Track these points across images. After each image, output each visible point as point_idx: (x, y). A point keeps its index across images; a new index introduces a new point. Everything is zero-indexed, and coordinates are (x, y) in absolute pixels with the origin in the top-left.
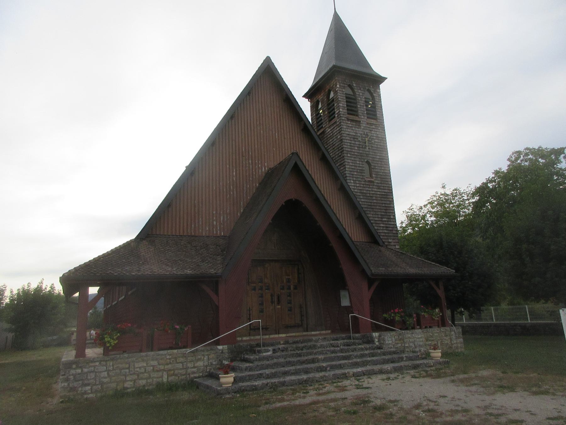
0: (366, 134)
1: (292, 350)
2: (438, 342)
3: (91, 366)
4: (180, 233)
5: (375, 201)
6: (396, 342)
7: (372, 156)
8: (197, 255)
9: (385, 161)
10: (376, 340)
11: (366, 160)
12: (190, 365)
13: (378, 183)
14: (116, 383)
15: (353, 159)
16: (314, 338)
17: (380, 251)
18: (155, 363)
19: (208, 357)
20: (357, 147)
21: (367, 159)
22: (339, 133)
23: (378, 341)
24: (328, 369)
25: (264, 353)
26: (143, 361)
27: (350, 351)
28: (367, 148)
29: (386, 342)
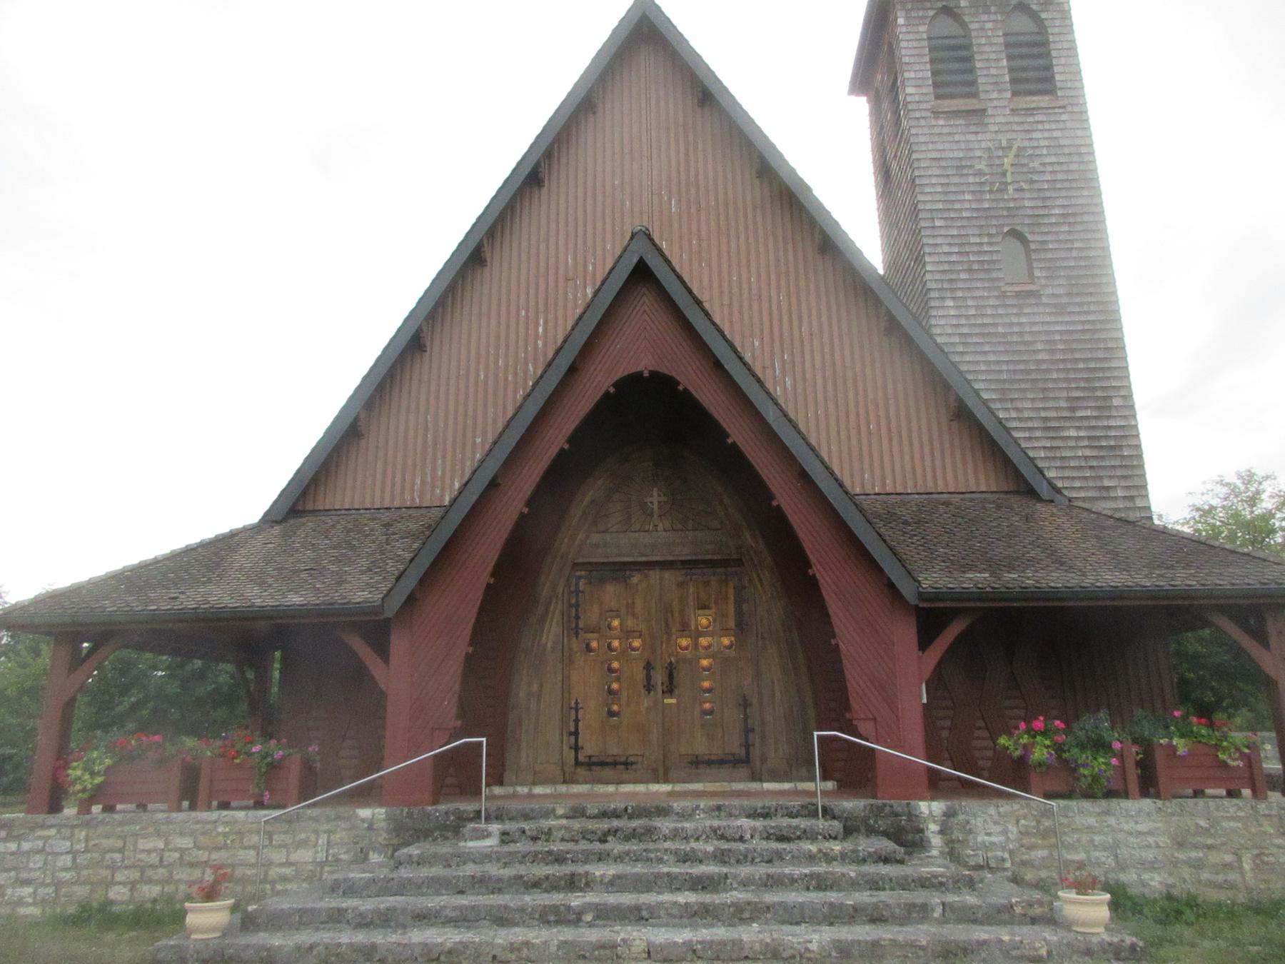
1: (566, 838)
2: (1240, 859)
3: (39, 838)
4: (383, 498)
6: (1026, 841)
10: (933, 827)
12: (278, 856)
14: (89, 887)
16: (677, 805)
18: (186, 842)
19: (329, 837)
21: (1008, 225)
23: (941, 832)
24: (588, 917)
25: (471, 840)
26: (158, 834)
27: (757, 860)
28: (1010, 188)
29: (975, 839)
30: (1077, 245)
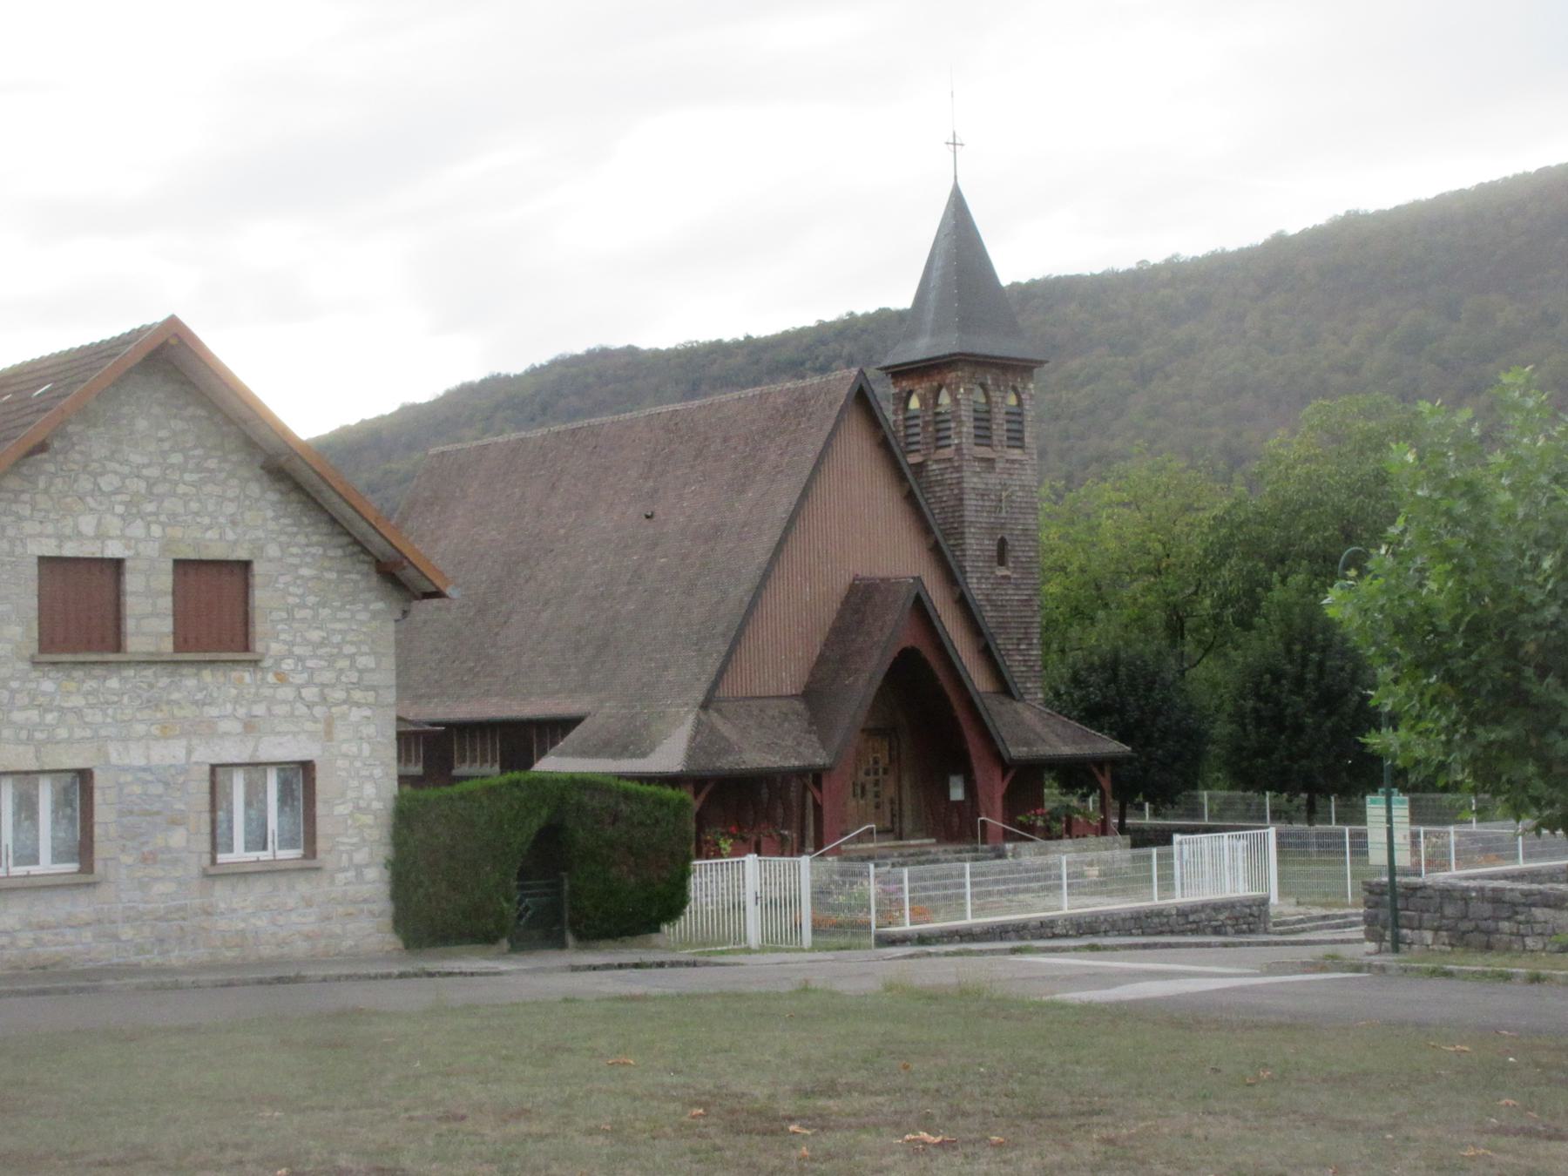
5: (1009, 614)
17: (1016, 712)
28: (1004, 511)
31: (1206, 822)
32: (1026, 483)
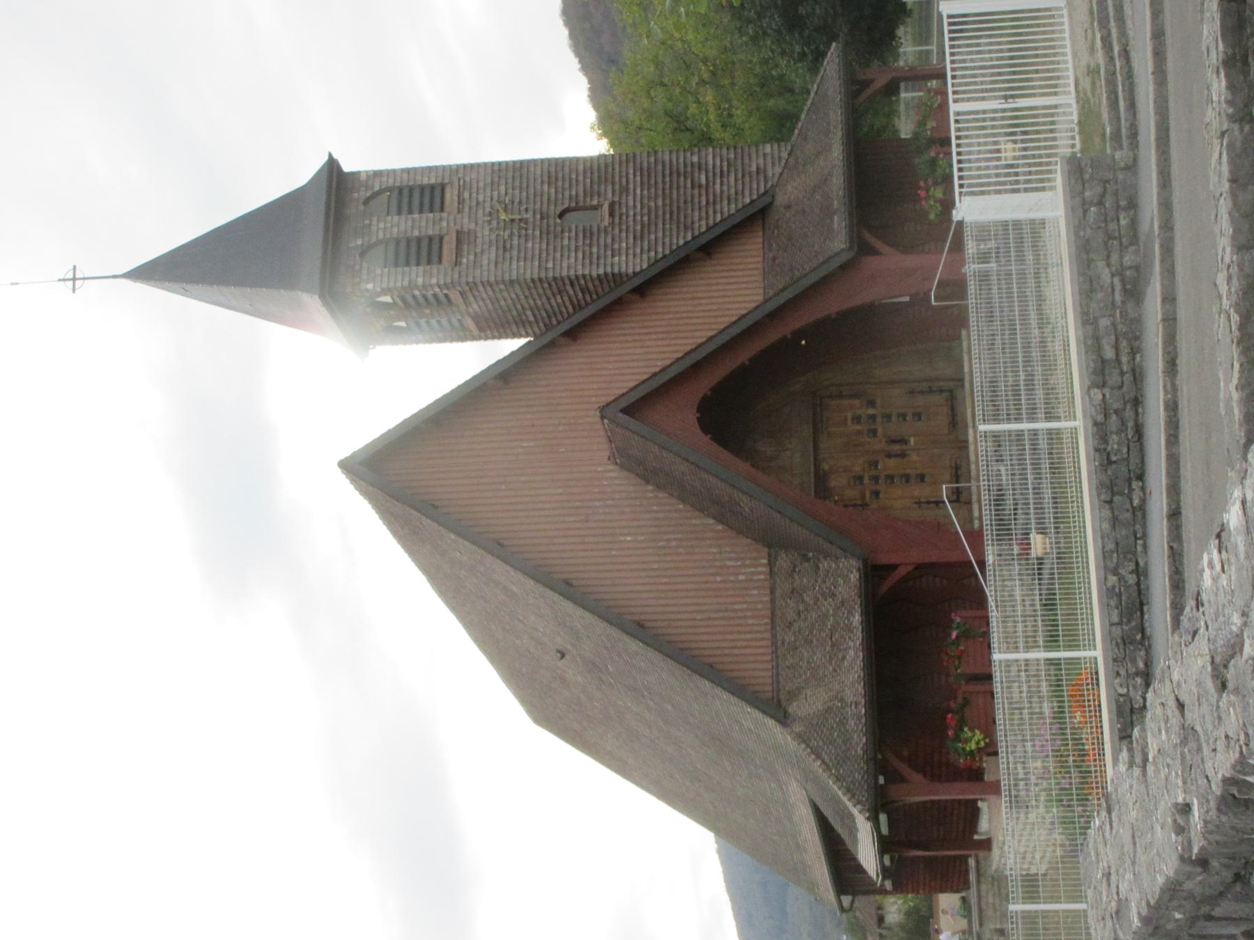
0: (489, 218)
5: (660, 203)
7: (545, 206)
8: (819, 608)
9: (553, 169)
11: (558, 221)
13: (614, 191)
15: (558, 255)
17: (788, 207)
20: (526, 241)
22: (491, 286)
28: (525, 216)
30: (574, 176)
31: (934, 48)
32: (489, 181)
